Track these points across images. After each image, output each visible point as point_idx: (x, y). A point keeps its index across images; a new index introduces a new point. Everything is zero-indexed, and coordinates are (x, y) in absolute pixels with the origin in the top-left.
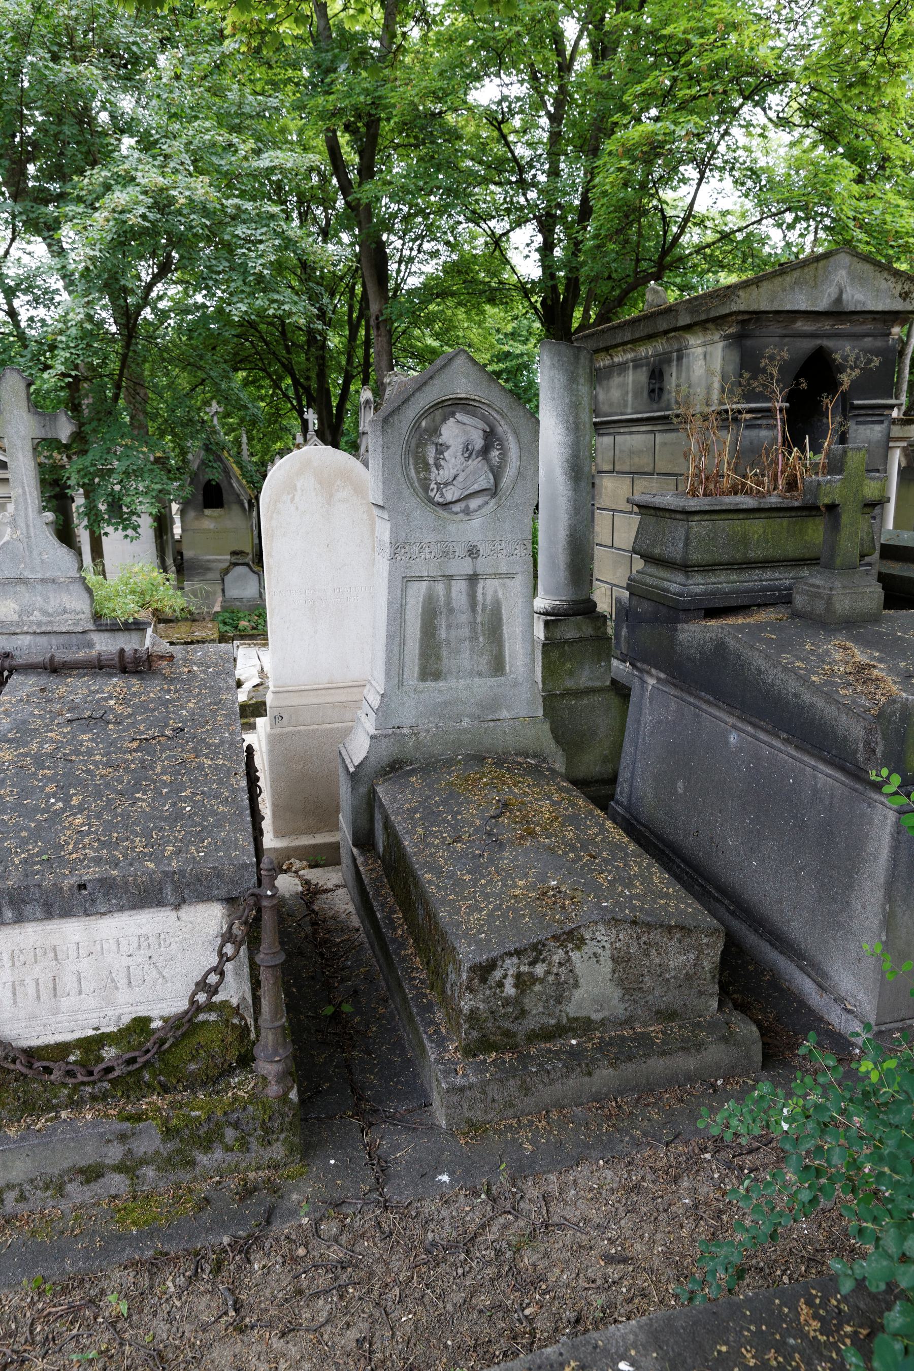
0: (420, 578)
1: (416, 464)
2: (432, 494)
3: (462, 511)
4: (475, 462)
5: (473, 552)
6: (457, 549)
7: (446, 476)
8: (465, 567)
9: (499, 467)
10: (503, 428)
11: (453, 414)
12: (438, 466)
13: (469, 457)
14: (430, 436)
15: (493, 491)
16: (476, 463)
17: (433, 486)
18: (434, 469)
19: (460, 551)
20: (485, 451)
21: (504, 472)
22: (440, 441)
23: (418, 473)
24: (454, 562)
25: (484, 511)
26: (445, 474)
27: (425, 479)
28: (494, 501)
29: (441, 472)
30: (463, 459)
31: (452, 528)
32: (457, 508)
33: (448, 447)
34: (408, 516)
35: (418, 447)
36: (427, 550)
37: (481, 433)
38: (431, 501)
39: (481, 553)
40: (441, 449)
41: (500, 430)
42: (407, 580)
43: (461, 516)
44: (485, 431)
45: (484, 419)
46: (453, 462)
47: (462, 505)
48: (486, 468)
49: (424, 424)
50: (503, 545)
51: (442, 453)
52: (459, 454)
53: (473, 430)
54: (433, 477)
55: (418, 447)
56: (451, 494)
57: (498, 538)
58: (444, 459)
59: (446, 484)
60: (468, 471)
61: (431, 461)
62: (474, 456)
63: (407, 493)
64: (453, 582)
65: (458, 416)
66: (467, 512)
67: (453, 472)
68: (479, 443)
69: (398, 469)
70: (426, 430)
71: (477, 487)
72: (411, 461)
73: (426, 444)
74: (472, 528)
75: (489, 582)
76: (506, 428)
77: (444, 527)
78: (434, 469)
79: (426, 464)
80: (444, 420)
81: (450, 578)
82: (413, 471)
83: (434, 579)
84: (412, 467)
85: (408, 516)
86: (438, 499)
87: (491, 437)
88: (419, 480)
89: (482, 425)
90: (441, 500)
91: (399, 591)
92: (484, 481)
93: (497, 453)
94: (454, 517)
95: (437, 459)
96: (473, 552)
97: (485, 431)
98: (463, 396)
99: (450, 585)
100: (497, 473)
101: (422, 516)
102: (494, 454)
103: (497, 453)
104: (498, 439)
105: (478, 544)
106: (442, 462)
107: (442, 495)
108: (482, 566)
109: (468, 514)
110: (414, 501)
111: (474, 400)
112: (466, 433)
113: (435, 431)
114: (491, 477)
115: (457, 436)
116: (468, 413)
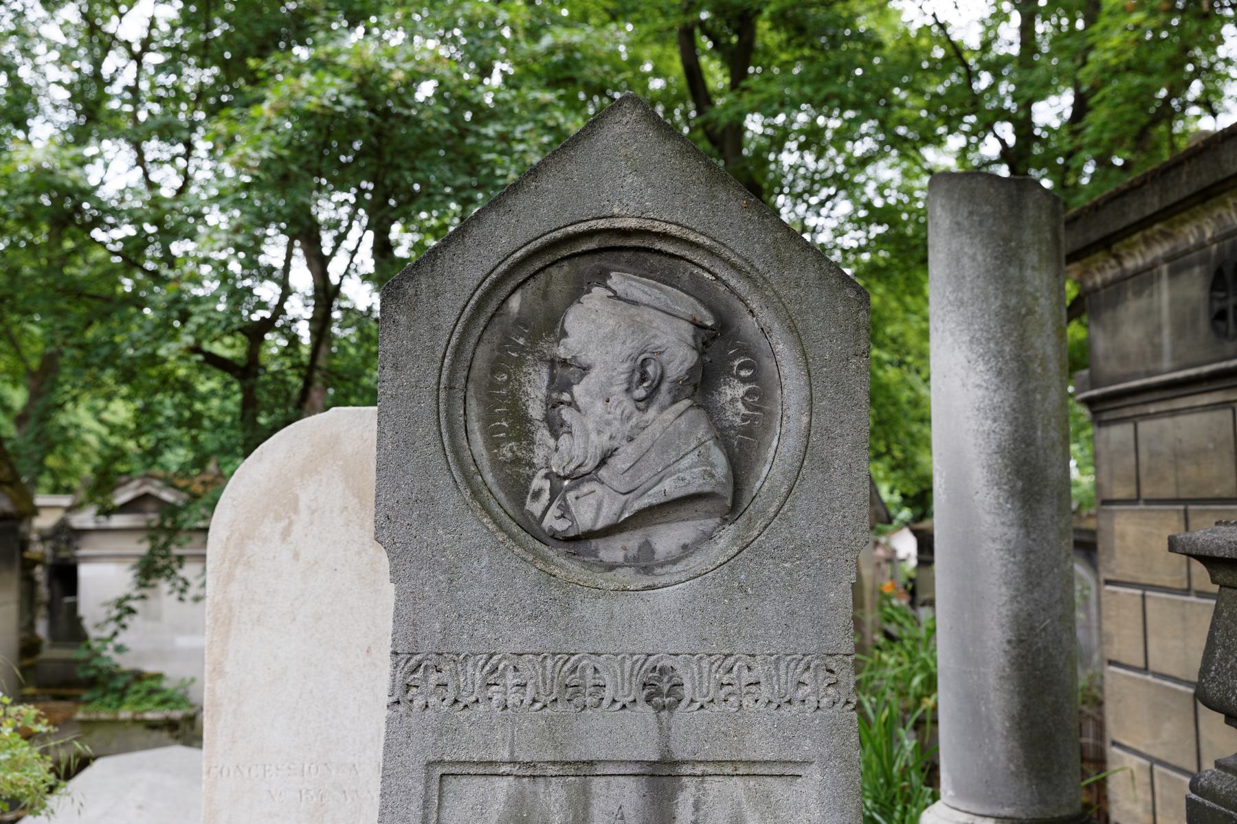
0: (488, 768)
1: (488, 419)
2: (536, 508)
3: (629, 562)
4: (669, 415)
5: (660, 690)
6: (606, 678)
7: (578, 452)
8: (637, 734)
9: (748, 432)
10: (757, 319)
11: (602, 277)
12: (556, 427)
13: (649, 399)
14: (534, 338)
15: (731, 501)
16: (667, 418)
17: (538, 482)
18: (542, 434)
19: (618, 682)
20: (701, 384)
21: (762, 445)
22: (561, 352)
23: (493, 443)
24: (598, 720)
25: (697, 562)
26: (575, 449)
27: (516, 461)
28: (730, 530)
29: (564, 440)
30: (629, 406)
31: (590, 611)
32: (613, 550)
33: (585, 370)
34: (451, 572)
35: (494, 371)
36: (511, 679)
37: (687, 330)
38: (532, 527)
39: (687, 691)
40: (564, 374)
41: (749, 325)
42: (443, 773)
43: (627, 576)
44: (699, 326)
45: (698, 290)
46: (599, 413)
47: (630, 542)
48: (702, 431)
49: (515, 303)
50: (759, 671)
51: (567, 386)
52: (618, 389)
53: (659, 320)
54: (539, 457)
55: (494, 371)
56: (592, 507)
57: (741, 647)
58: (572, 404)
59: (578, 478)
60: (644, 439)
61: (536, 411)
62: (664, 396)
63: (451, 499)
64: (598, 784)
65: (616, 280)
66: (645, 562)
67: (600, 442)
68: (679, 357)
69: (426, 429)
70: (520, 322)
71: (670, 488)
72: (474, 408)
73: (520, 362)
74: (657, 614)
75: (714, 786)
76: (766, 317)
77: (567, 609)
78: (542, 434)
79: (520, 420)
80: (577, 293)
81: (585, 768)
82: (478, 439)
83: (532, 771)
84: (475, 426)
85: (451, 572)
86: (552, 521)
87: (718, 344)
88: (497, 464)
89: (687, 305)
90: (561, 526)
91: (415, 807)
92: (696, 467)
93: (741, 390)
94: (601, 579)
95: (553, 405)
96: (660, 690)
97: (699, 326)
98: (632, 223)
99: (585, 792)
100: (741, 455)
101: (494, 572)
102: (733, 393)
103: (741, 390)
104: (744, 351)
105: (677, 662)
106: (566, 414)
107: (565, 512)
108: (689, 733)
109: (647, 570)
110: (474, 527)
111: (664, 236)
112: (638, 327)
113: (550, 325)
114: (718, 457)
115: (612, 336)
116: (650, 274)
